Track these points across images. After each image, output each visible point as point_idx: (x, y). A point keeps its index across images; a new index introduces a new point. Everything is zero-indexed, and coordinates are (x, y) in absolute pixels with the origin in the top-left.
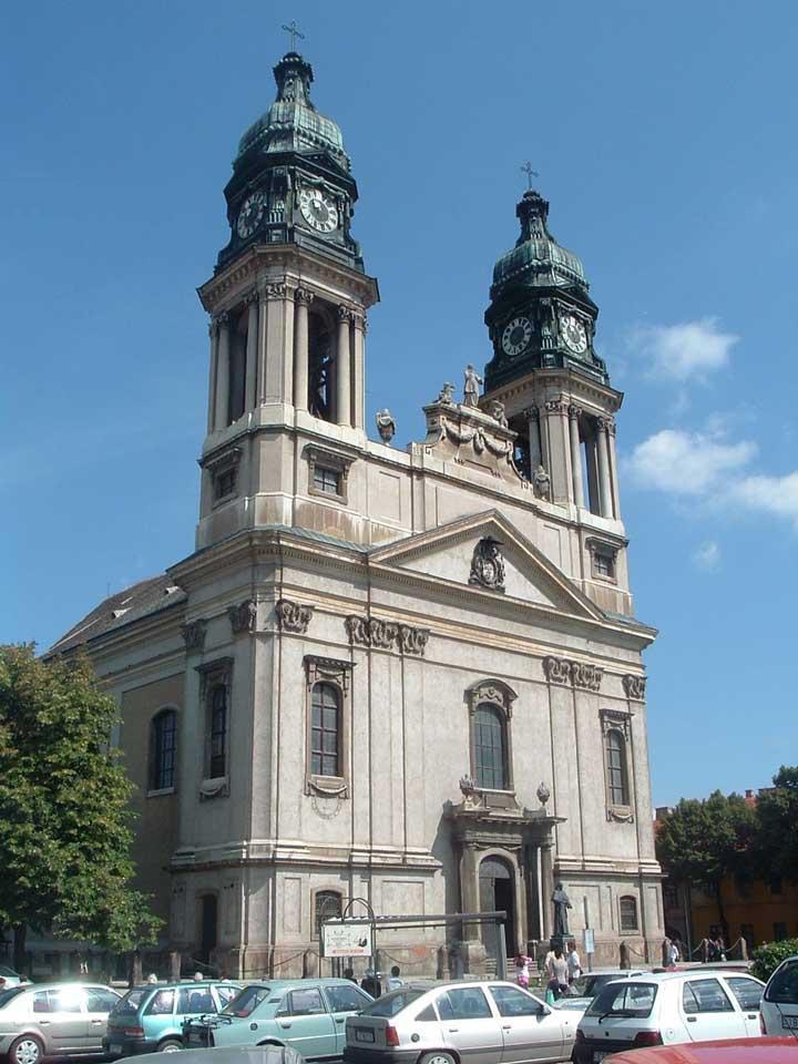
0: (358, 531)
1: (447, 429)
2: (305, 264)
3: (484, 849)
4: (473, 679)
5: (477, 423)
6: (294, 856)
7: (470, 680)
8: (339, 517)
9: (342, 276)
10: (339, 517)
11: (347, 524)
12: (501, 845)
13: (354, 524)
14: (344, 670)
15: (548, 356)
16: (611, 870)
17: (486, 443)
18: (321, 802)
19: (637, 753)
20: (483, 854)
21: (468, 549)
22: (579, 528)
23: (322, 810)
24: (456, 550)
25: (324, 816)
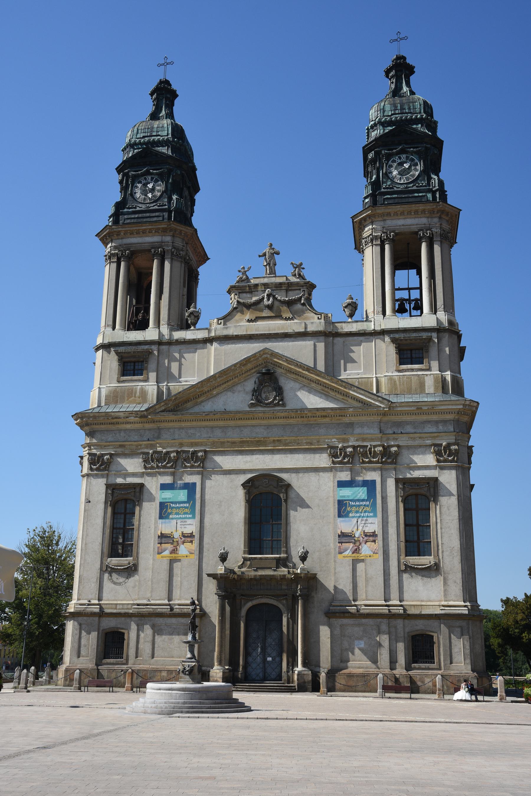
0: (153, 394)
1: (238, 302)
2: (122, 234)
3: (251, 600)
4: (249, 476)
5: (266, 286)
6: (88, 609)
7: (244, 478)
8: (138, 391)
9: (150, 229)
10: (138, 391)
11: (144, 394)
12: (267, 596)
13: (150, 392)
14: (135, 489)
15: (367, 200)
16: (397, 611)
17: (275, 298)
18: (115, 576)
19: (444, 510)
20: (250, 604)
21: (250, 385)
22: (383, 333)
23: (115, 580)
24: (239, 388)
25: (115, 583)
